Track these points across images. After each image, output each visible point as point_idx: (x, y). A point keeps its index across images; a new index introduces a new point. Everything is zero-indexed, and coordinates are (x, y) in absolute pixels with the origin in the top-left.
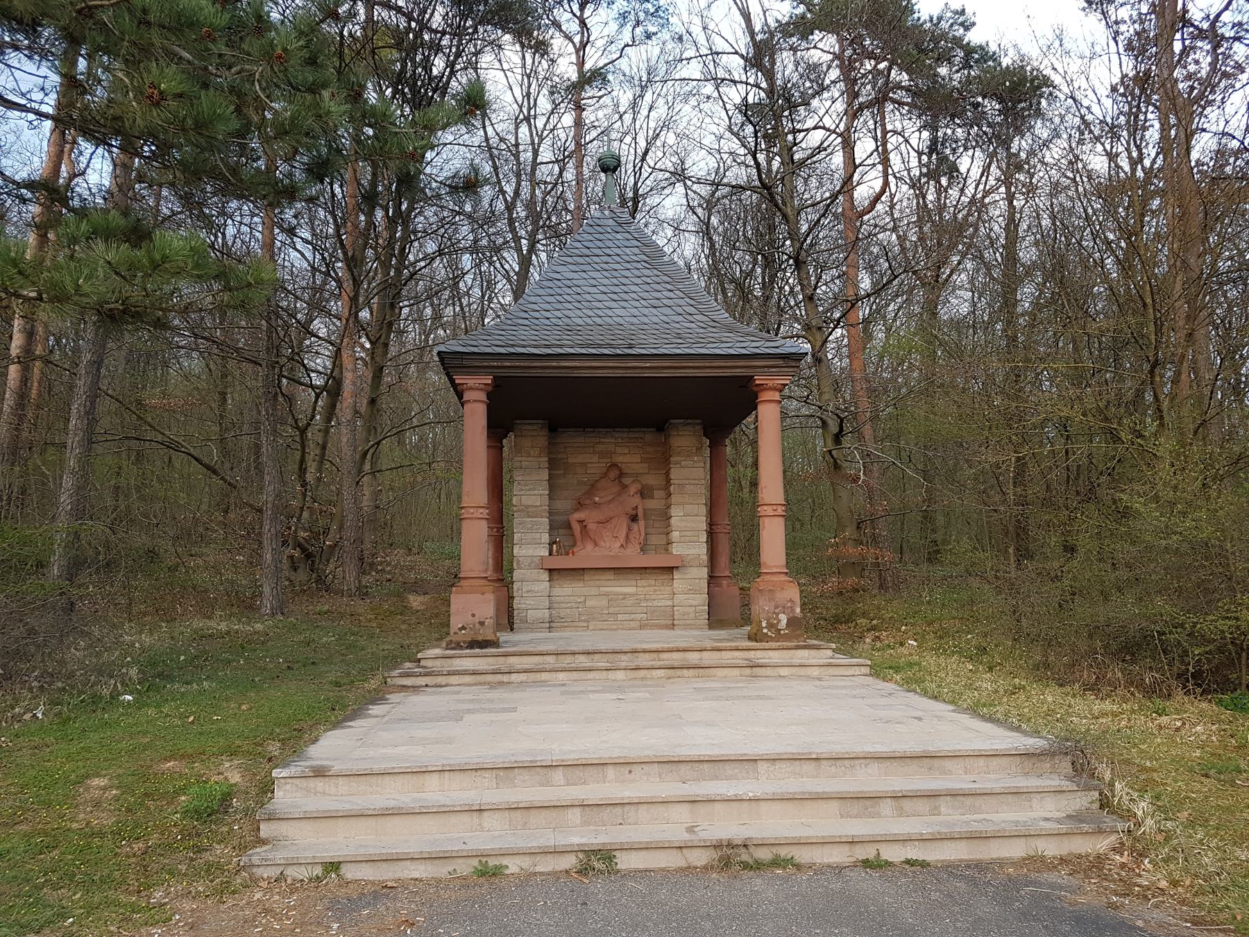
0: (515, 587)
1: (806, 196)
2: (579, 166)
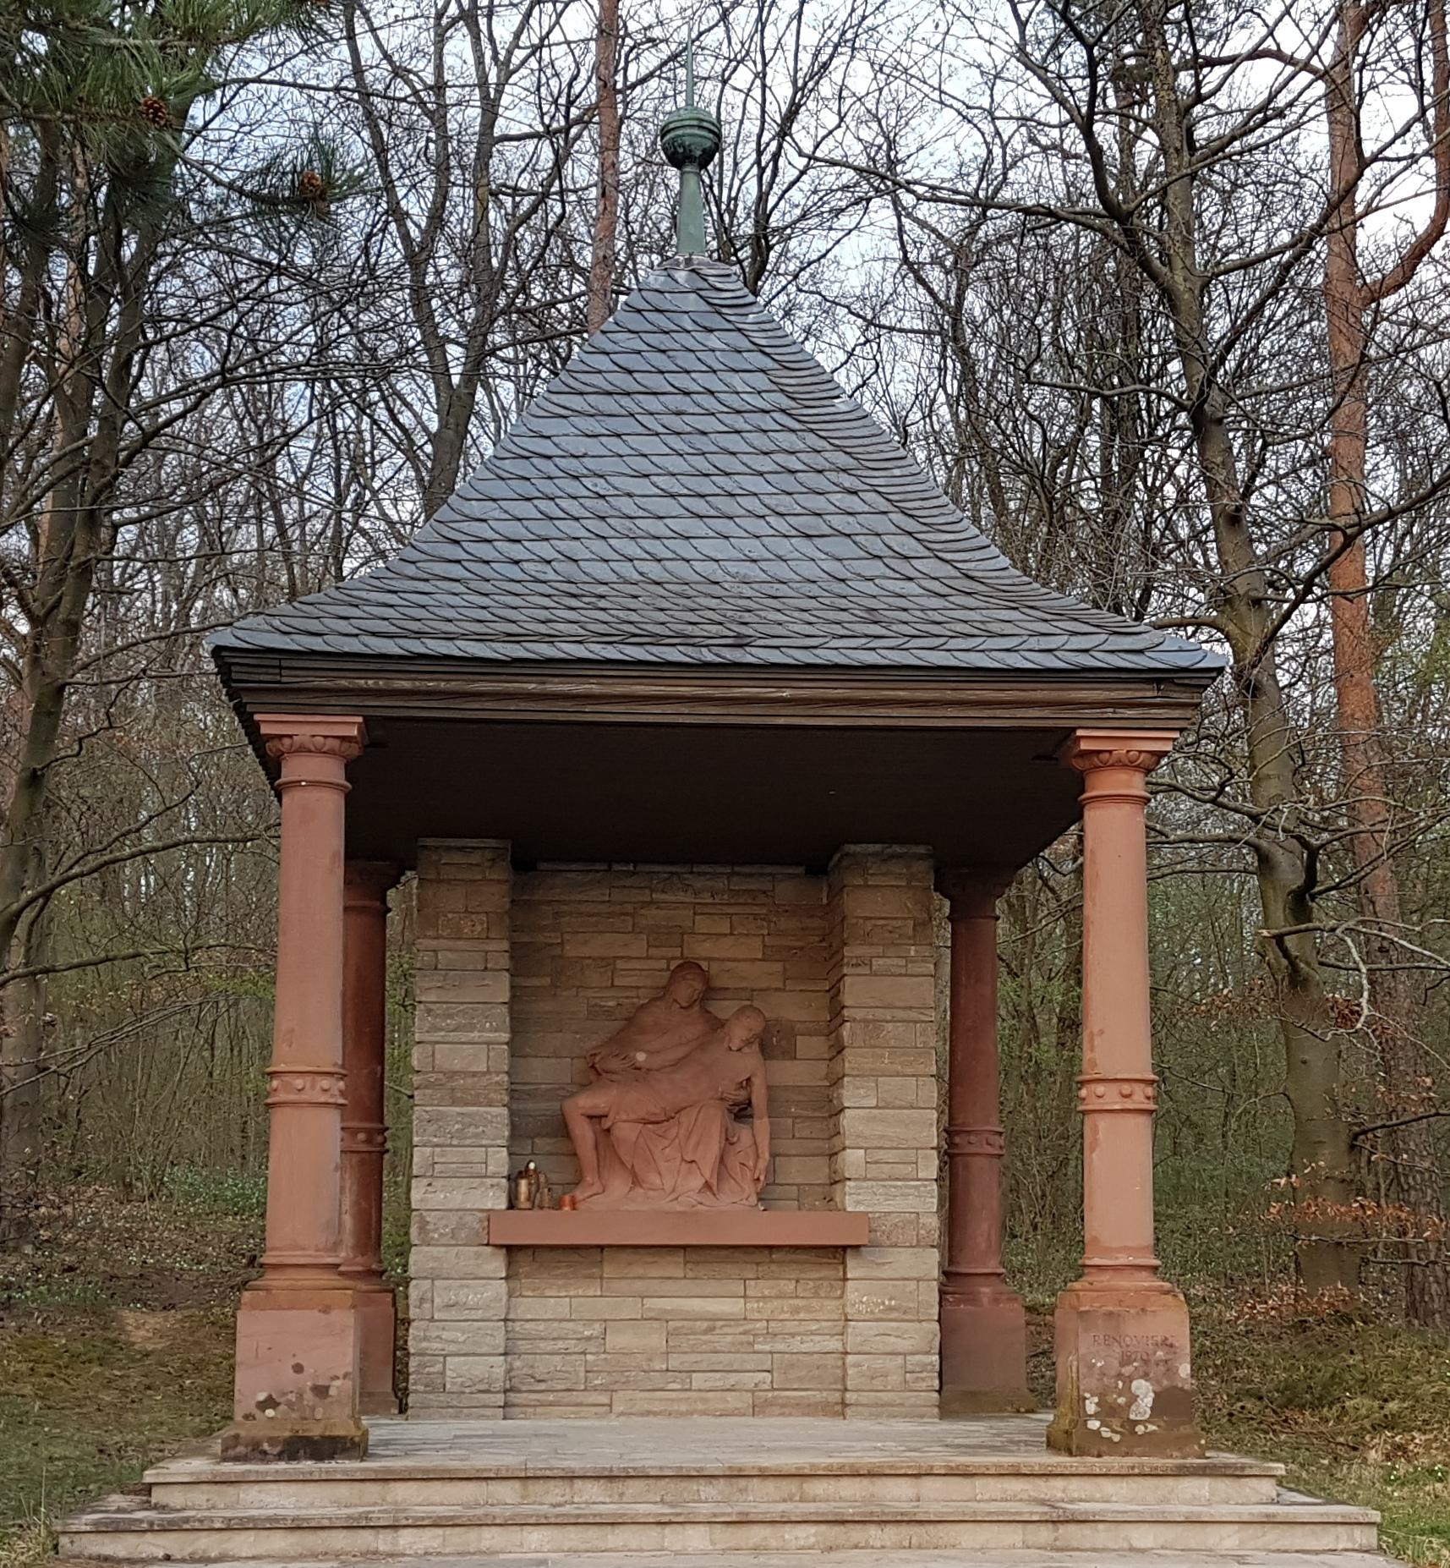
0: (414, 1293)
1: (1227, 240)
2: (608, 147)
